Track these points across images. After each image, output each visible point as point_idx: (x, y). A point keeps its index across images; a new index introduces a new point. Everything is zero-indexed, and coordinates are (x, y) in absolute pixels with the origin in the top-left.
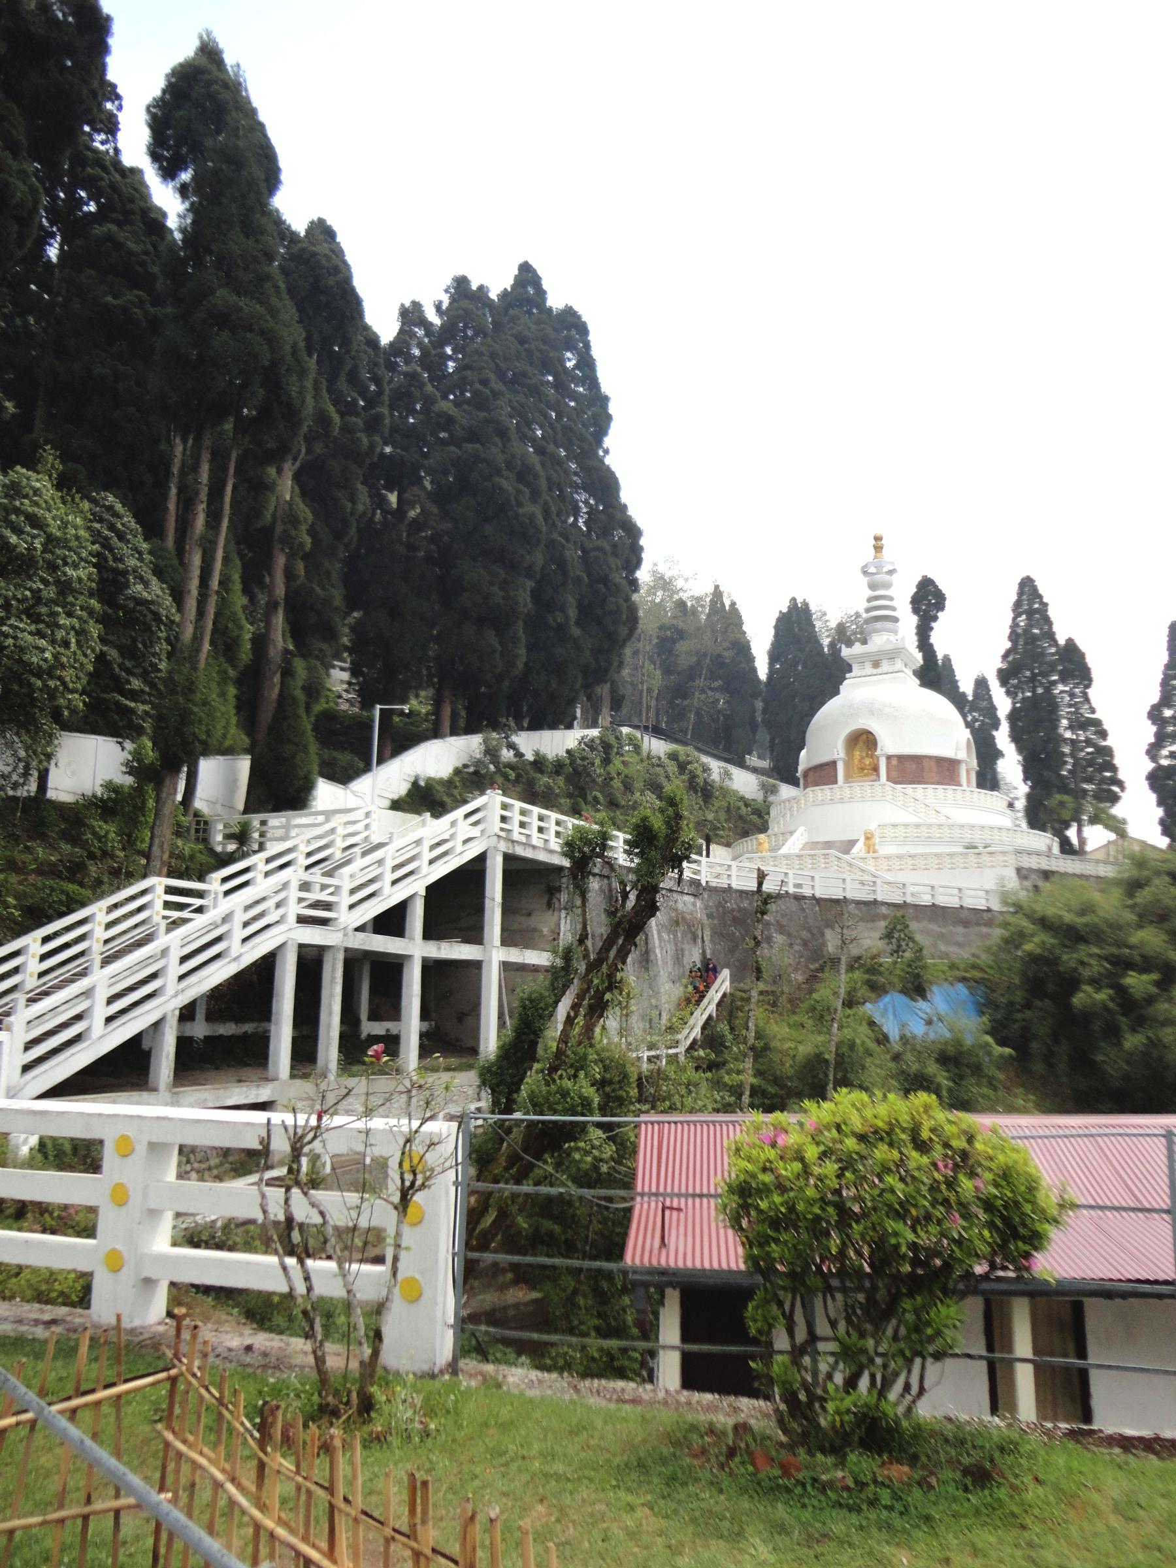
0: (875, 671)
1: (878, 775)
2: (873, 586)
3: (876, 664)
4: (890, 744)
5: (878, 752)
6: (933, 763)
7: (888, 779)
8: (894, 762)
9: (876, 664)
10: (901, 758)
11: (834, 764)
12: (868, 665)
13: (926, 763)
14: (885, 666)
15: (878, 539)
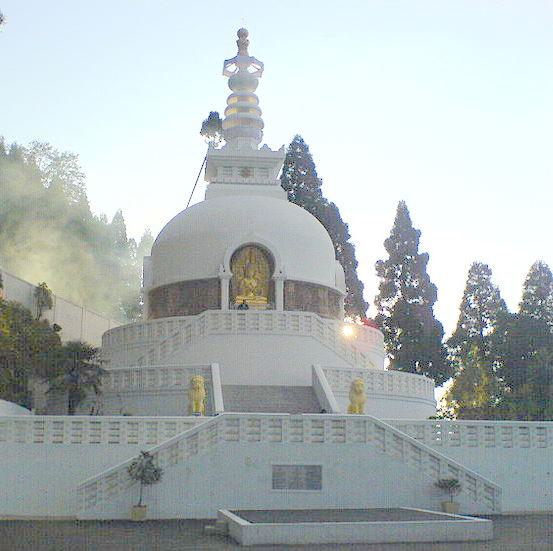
0: (247, 180)
1: (271, 298)
2: (231, 84)
3: (246, 172)
4: (289, 268)
5: (276, 274)
6: (326, 296)
7: (285, 309)
8: (292, 288)
9: (246, 172)
10: (298, 284)
11: (219, 281)
12: (236, 172)
13: (321, 294)
14: (257, 176)
15: (242, 34)
